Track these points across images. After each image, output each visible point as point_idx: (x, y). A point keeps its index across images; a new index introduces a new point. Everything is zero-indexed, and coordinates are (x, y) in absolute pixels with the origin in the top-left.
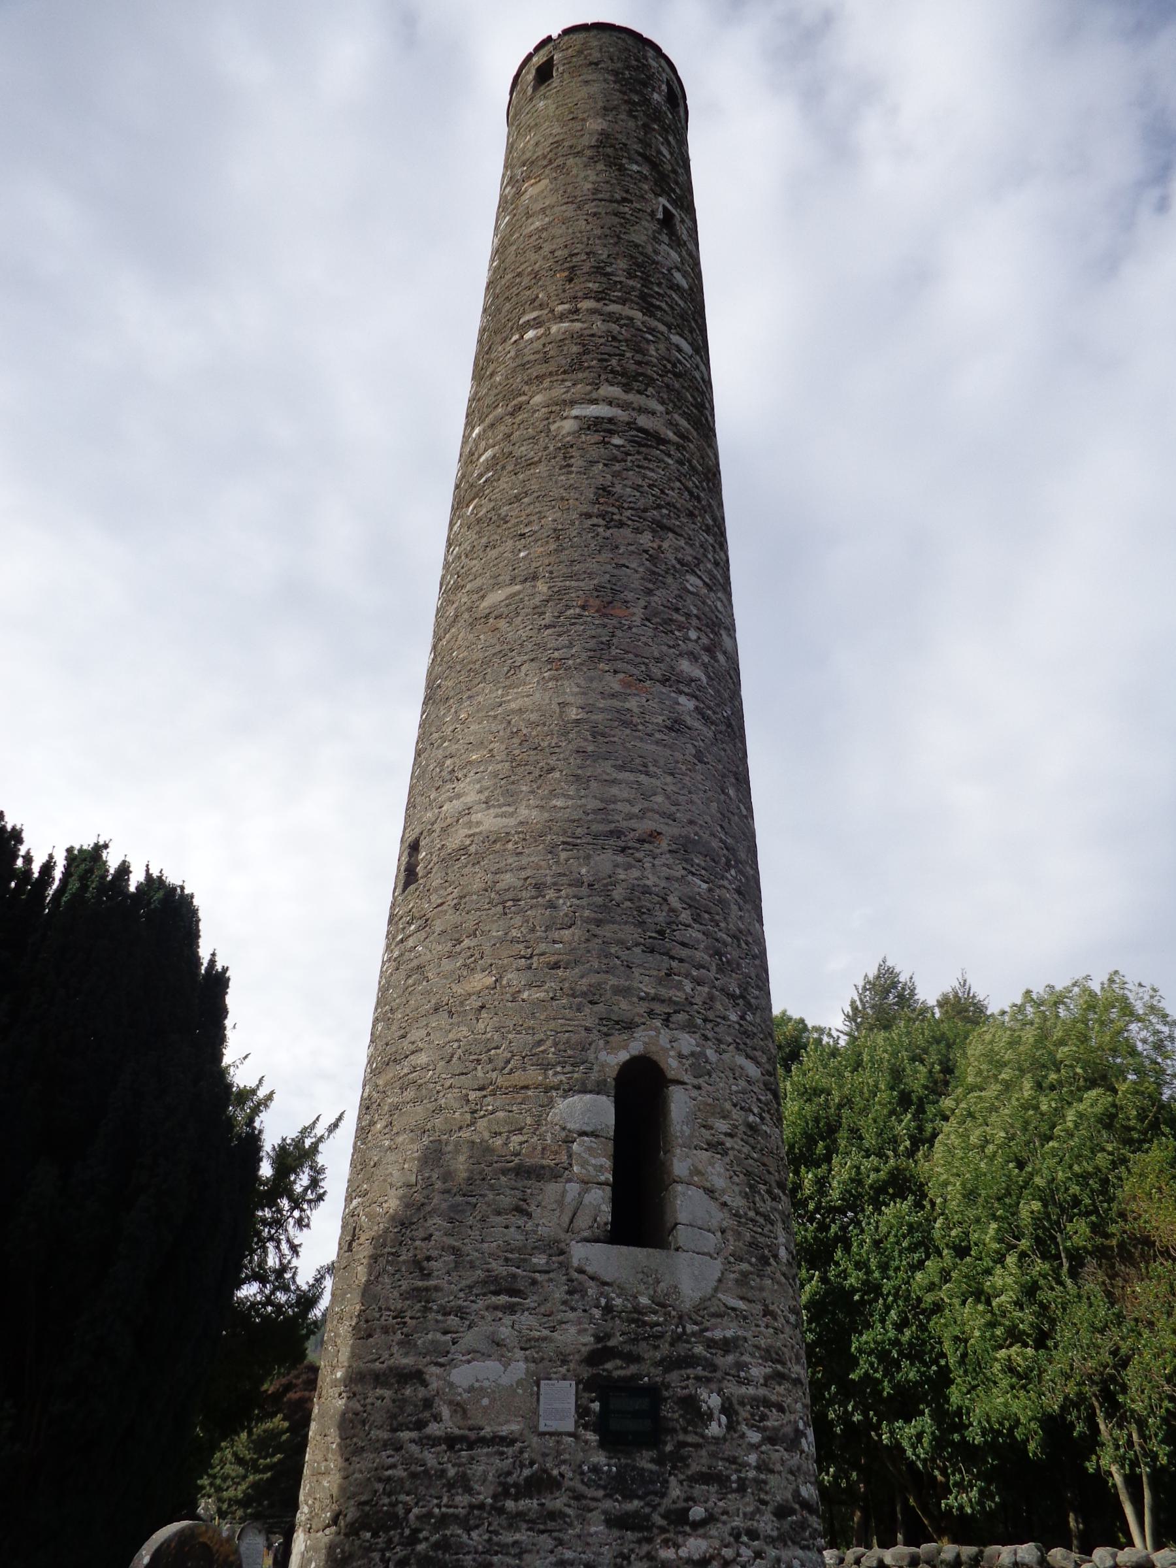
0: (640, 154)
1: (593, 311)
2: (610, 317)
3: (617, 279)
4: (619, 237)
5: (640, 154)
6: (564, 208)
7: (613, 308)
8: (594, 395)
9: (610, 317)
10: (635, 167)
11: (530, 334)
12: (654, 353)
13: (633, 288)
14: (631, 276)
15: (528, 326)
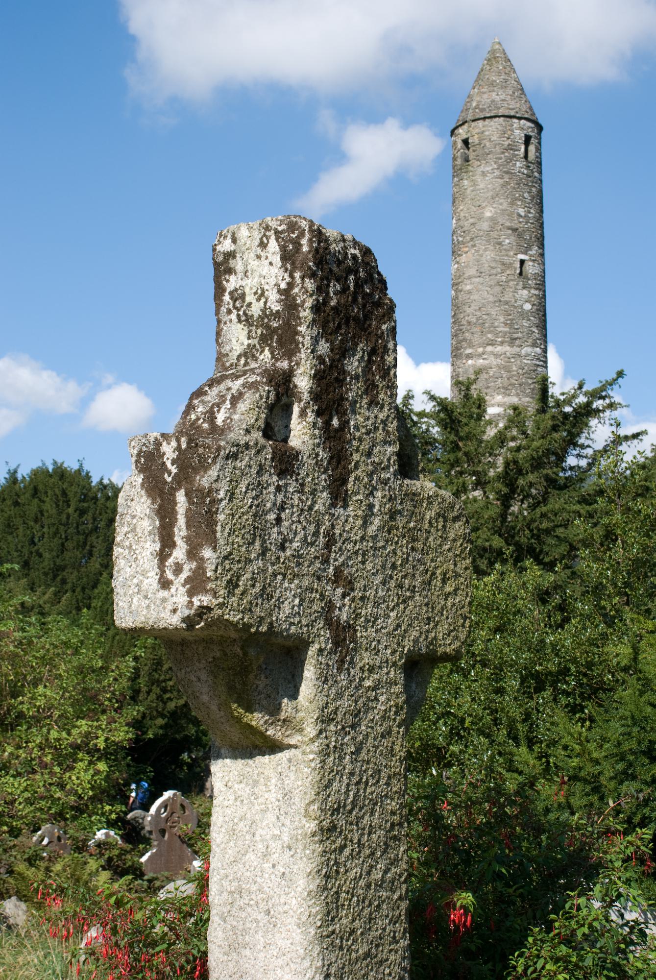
0: (509, 228)
1: (492, 353)
2: (497, 356)
3: (499, 329)
4: (500, 301)
5: (509, 228)
6: (477, 280)
7: (499, 349)
8: (493, 402)
9: (497, 356)
10: (507, 241)
11: (470, 362)
12: (514, 368)
13: (506, 333)
14: (506, 324)
15: (469, 356)
